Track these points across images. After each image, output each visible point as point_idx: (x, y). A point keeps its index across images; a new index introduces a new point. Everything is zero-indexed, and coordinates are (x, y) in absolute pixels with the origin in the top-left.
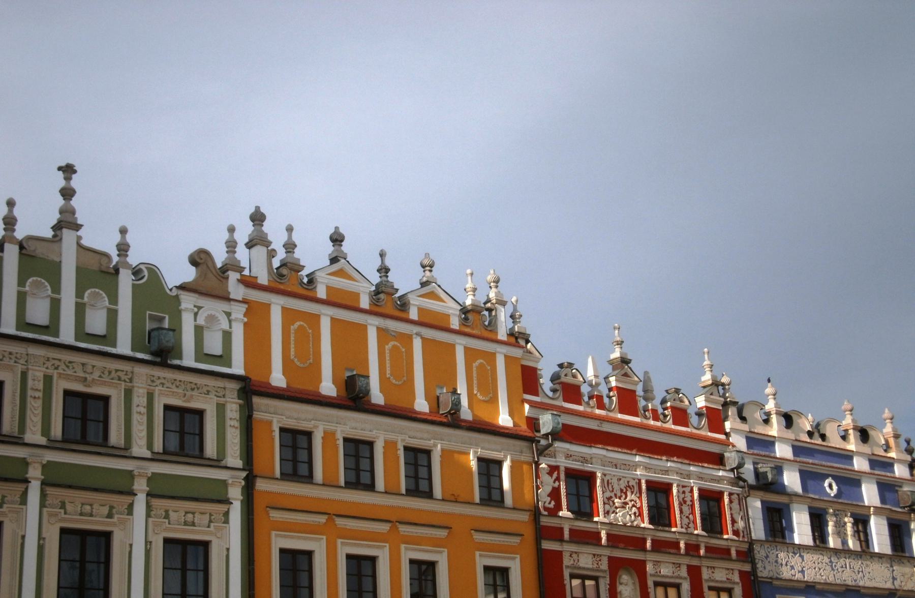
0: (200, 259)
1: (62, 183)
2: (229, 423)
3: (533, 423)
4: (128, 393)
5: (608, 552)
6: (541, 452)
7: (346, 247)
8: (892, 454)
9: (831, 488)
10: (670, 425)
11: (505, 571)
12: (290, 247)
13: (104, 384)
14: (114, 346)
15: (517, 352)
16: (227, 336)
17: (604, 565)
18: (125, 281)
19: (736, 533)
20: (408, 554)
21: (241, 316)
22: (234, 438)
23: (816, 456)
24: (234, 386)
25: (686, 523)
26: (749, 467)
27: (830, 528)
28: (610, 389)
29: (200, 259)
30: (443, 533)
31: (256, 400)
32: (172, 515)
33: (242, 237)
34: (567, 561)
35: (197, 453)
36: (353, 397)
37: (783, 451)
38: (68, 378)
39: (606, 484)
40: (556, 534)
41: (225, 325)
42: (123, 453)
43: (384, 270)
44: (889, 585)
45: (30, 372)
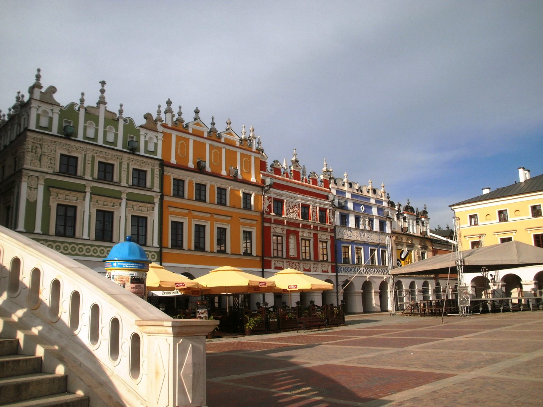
0: (148, 117)
1: (101, 88)
2: (155, 175)
3: (263, 181)
4: (121, 163)
5: (286, 228)
6: (266, 192)
7: (200, 115)
8: (383, 198)
9: (362, 209)
10: (311, 185)
11: (250, 233)
12: (180, 114)
13: (112, 160)
14: (116, 146)
15: (259, 156)
16: (156, 145)
17: (285, 232)
18: (121, 123)
19: (330, 223)
20: (217, 225)
21: (161, 138)
22: (157, 181)
23: (359, 198)
24: (158, 163)
25: (314, 219)
26: (336, 200)
27: (361, 222)
28: (291, 171)
29: (148, 117)
30: (230, 218)
31: (165, 168)
32: (135, 207)
33: (163, 109)
34: (272, 230)
35: (144, 186)
36: (200, 169)
37: (348, 196)
38: (100, 157)
39: (288, 204)
40: (269, 221)
41: (155, 141)
42: (118, 184)
43: (213, 124)
44: (378, 242)
45: (87, 155)
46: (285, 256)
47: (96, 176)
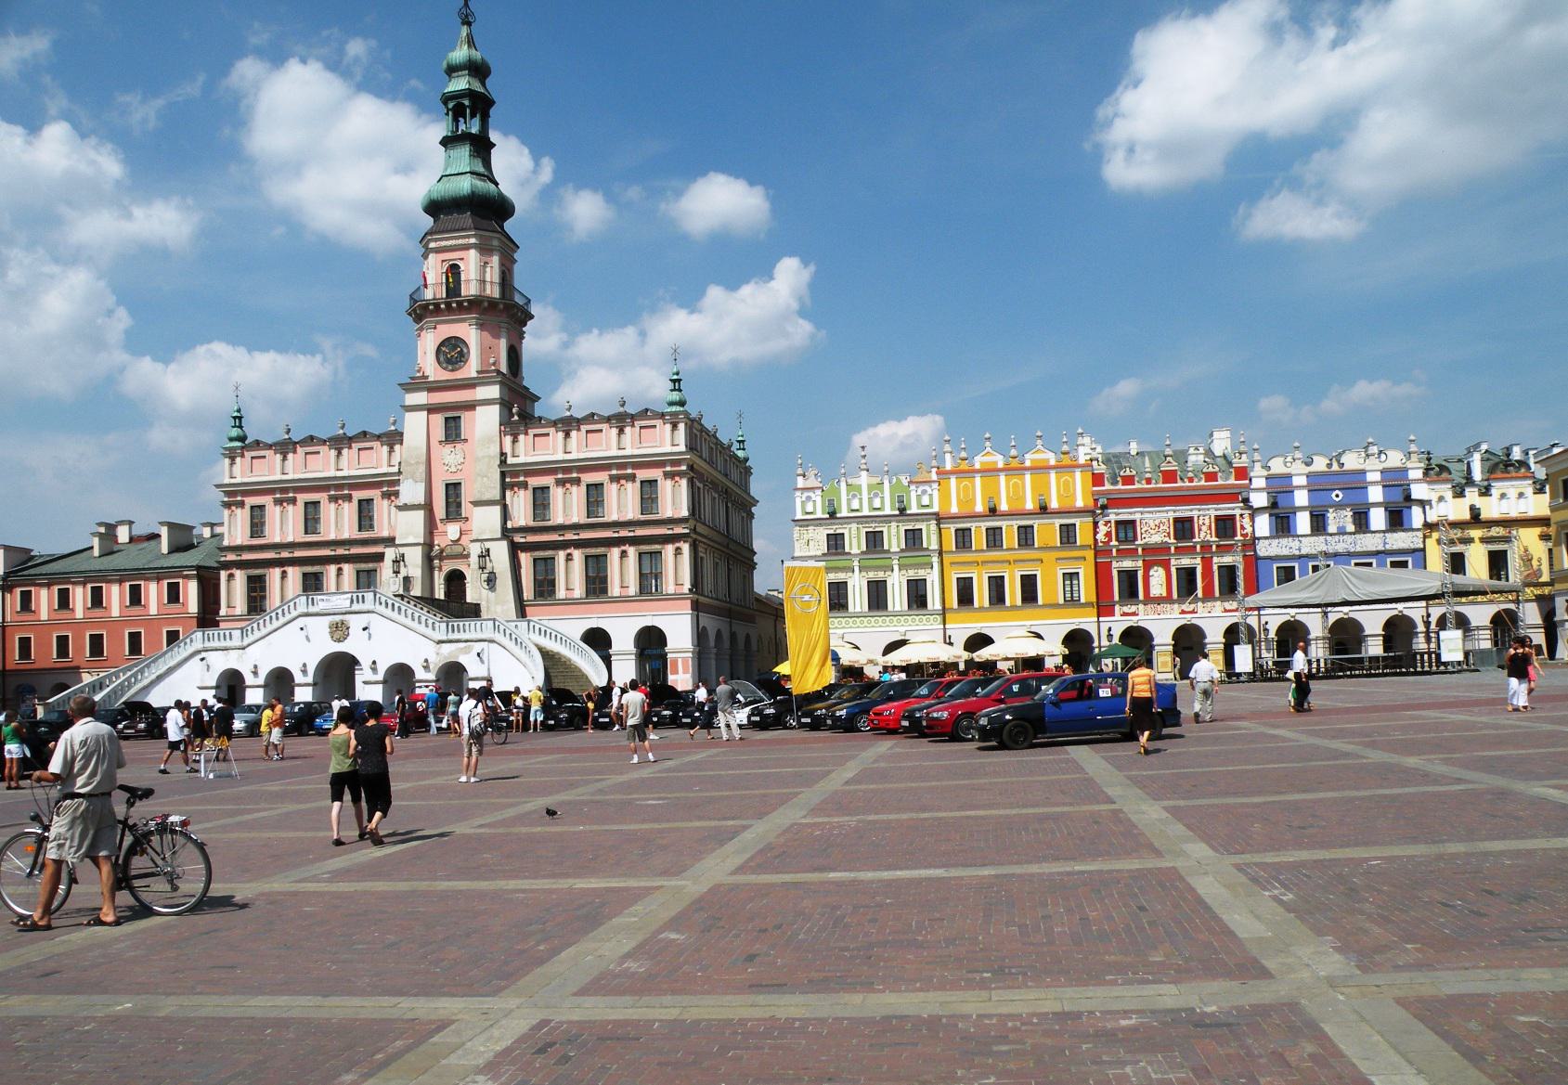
17: (1140, 563)
22: (934, 538)
25: (1205, 532)
46: (1141, 596)
47: (864, 548)
